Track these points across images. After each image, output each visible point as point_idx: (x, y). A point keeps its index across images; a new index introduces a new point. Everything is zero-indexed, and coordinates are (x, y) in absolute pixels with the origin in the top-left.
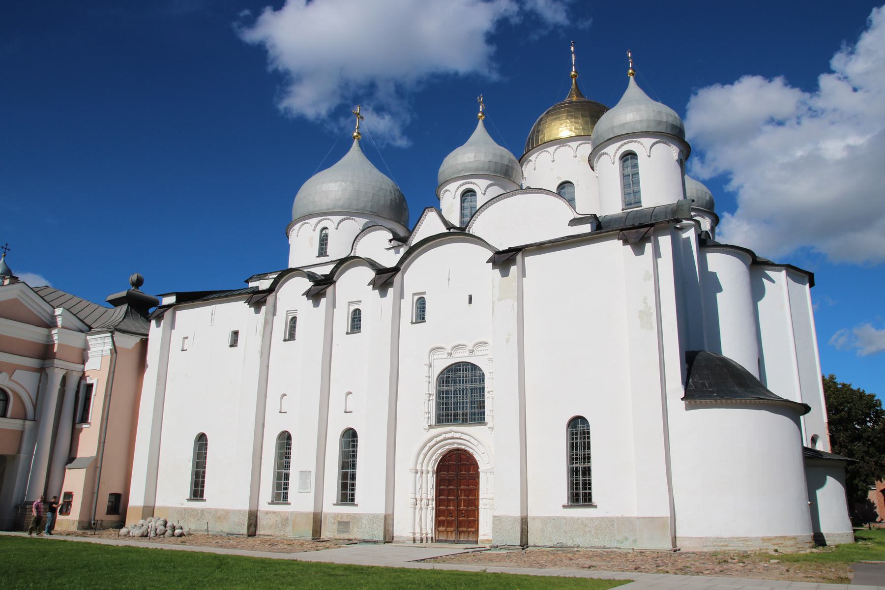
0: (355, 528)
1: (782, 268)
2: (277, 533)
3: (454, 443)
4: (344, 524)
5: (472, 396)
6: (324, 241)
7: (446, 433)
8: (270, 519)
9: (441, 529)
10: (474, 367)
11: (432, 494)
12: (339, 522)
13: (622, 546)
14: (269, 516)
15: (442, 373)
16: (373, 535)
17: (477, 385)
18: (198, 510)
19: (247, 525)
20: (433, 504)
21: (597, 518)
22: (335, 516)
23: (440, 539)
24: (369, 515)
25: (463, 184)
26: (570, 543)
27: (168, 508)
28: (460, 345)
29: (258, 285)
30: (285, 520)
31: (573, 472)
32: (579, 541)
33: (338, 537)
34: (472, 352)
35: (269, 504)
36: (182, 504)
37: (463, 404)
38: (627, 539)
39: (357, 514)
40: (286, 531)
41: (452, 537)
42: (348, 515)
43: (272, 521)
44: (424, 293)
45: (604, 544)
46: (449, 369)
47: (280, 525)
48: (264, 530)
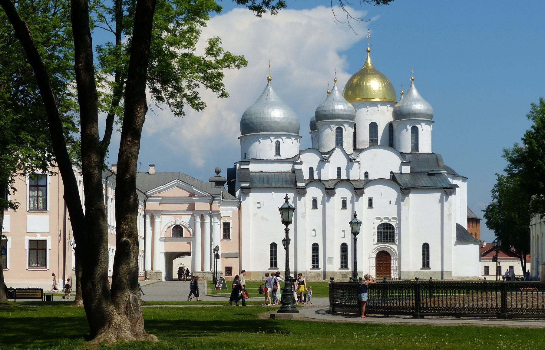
1: (461, 178)
4: (344, 275)
6: (278, 147)
7: (382, 246)
9: (378, 276)
10: (390, 225)
11: (375, 265)
12: (342, 275)
13: (438, 279)
14: (311, 273)
15: (379, 226)
17: (392, 231)
22: (340, 273)
26: (423, 279)
27: (258, 272)
28: (386, 217)
30: (319, 275)
31: (424, 259)
34: (390, 220)
36: (266, 270)
42: (345, 272)
46: (381, 225)
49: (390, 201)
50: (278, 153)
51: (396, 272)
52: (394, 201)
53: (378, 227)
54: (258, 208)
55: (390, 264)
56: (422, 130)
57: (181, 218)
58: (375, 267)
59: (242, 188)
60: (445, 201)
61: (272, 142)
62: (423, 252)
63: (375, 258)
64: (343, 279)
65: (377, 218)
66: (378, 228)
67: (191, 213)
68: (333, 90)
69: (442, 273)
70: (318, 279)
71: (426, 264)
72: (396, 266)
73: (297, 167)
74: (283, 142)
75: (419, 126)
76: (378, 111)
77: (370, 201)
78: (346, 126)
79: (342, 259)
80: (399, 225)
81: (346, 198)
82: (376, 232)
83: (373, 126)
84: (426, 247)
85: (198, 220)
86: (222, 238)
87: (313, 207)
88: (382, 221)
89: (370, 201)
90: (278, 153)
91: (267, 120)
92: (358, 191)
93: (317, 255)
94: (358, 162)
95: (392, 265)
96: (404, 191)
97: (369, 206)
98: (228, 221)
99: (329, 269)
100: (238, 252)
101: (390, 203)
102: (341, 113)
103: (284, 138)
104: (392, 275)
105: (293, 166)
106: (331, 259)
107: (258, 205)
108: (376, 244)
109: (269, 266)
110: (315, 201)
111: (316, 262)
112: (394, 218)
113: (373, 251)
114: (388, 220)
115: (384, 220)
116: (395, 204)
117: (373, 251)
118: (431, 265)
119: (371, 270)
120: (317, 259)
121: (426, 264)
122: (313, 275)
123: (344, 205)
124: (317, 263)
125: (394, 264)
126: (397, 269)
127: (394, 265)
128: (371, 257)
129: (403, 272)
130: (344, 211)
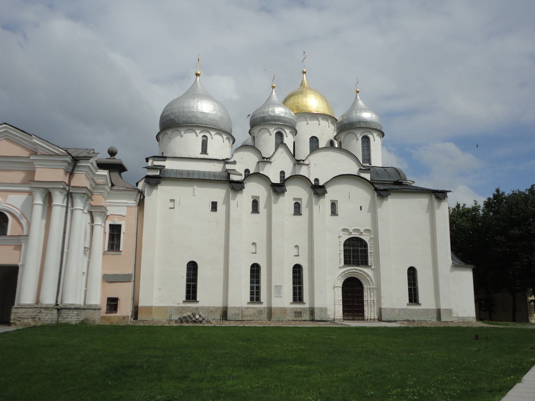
0: (305, 315)
2: (255, 319)
3: (353, 274)
4: (298, 313)
5: (356, 253)
8: (250, 311)
9: (346, 314)
11: (341, 299)
12: (295, 312)
14: (249, 310)
15: (346, 241)
16: (322, 317)
18: (194, 307)
19: (241, 314)
20: (342, 303)
21: (422, 309)
22: (292, 309)
23: (345, 319)
24: (319, 308)
25: (279, 128)
26: (411, 319)
27: (166, 307)
28: (356, 229)
29: (165, 165)
30: (260, 312)
31: (410, 290)
32: (415, 318)
33: (295, 319)
34: (362, 233)
35: (248, 303)
36: (179, 304)
37: (356, 257)
38: (434, 317)
39: (306, 308)
40: (261, 318)
41: (350, 318)
42: (300, 308)
43: (251, 312)
44: (337, 201)
45: (425, 319)
46: (349, 240)
47: (257, 315)
48: (246, 317)
49: (361, 207)
50: (204, 150)
51: (372, 309)
52: (366, 207)
53: (344, 243)
54: (170, 208)
55: (362, 297)
56: (374, 141)
57: (5, 198)
58: (342, 302)
59: (147, 177)
60: (437, 209)
61: (197, 136)
62: (409, 280)
63: (341, 288)
64: (297, 319)
65: (345, 230)
66: (345, 245)
67: (28, 189)
68: (271, 93)
69: (439, 312)
70: (259, 318)
71: (413, 298)
72: (372, 299)
73: (228, 167)
74: (212, 138)
75: (370, 136)
76: (319, 125)
77: (334, 205)
78: (288, 131)
79: (294, 288)
80: (376, 239)
81: (301, 199)
82: (343, 249)
83: (314, 140)
84: (412, 272)
85: (39, 200)
86: (106, 249)
87: (253, 211)
88: (350, 233)
89: (334, 205)
90: (204, 150)
91: (192, 110)
92: (318, 191)
93: (258, 282)
94: (307, 165)
95: (365, 299)
96: (382, 193)
97: (331, 213)
98: (117, 222)
99: (276, 303)
100: (131, 272)
101: (361, 209)
102: (283, 115)
103: (213, 133)
104: (366, 314)
105: (224, 166)
106: (279, 288)
107: (171, 205)
108: (344, 267)
109: (184, 298)
110: (255, 204)
111: (256, 292)
112: (367, 230)
113: (339, 278)
114: (358, 234)
115: (353, 233)
116: (368, 212)
117: (339, 278)
118: (421, 301)
119: (337, 306)
120: (258, 288)
121: (413, 298)
122: (252, 312)
123: (297, 208)
124: (258, 293)
125: (368, 297)
126: (374, 305)
127: (369, 299)
128: (337, 287)
129: (385, 309)
130: (298, 217)
